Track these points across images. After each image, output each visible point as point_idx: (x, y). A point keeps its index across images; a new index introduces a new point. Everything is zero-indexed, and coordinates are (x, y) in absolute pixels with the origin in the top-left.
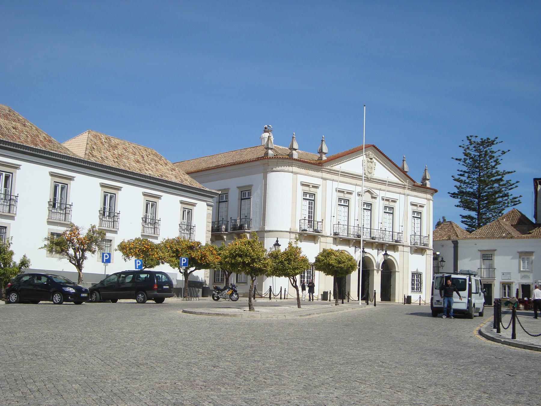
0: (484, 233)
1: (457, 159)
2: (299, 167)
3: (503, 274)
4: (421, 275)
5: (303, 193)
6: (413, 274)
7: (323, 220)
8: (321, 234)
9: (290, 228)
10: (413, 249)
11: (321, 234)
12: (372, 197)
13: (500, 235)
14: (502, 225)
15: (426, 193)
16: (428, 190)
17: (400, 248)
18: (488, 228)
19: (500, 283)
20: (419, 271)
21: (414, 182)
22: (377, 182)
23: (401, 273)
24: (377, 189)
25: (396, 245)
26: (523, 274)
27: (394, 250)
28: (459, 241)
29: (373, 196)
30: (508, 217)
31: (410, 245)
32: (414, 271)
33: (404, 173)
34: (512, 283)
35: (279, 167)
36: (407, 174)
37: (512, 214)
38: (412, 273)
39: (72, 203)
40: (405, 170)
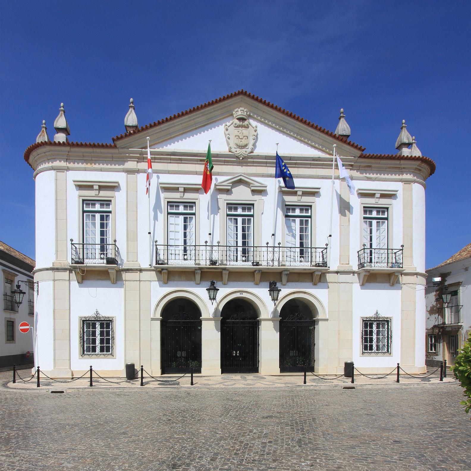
2: (67, 160)
4: (388, 321)
5: (362, 209)
6: (367, 323)
8: (166, 266)
9: (53, 263)
10: (362, 276)
11: (166, 266)
12: (254, 192)
15: (400, 170)
16: (403, 162)
17: (329, 277)
20: (383, 314)
22: (266, 163)
24: (263, 176)
27: (313, 281)
29: (252, 188)
31: (355, 268)
32: (368, 316)
38: (363, 321)
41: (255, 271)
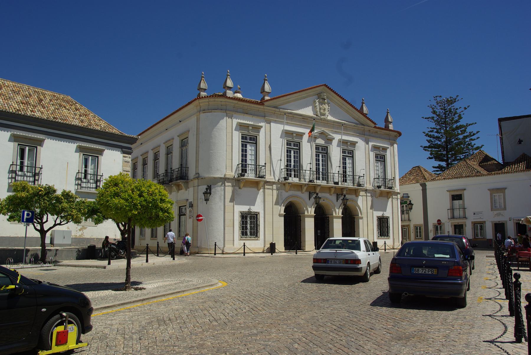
0: (452, 174)
1: (426, 118)
3: (474, 214)
7: (265, 164)
13: (468, 174)
14: (470, 165)
18: (455, 169)
19: (472, 223)
21: (375, 124)
23: (365, 219)
25: (358, 189)
26: (496, 212)
28: (426, 183)
30: (475, 158)
33: (364, 116)
34: (485, 222)
35: (245, 121)
36: (368, 116)
37: (479, 155)
39: (42, 166)
40: (364, 112)
41: (332, 187)
